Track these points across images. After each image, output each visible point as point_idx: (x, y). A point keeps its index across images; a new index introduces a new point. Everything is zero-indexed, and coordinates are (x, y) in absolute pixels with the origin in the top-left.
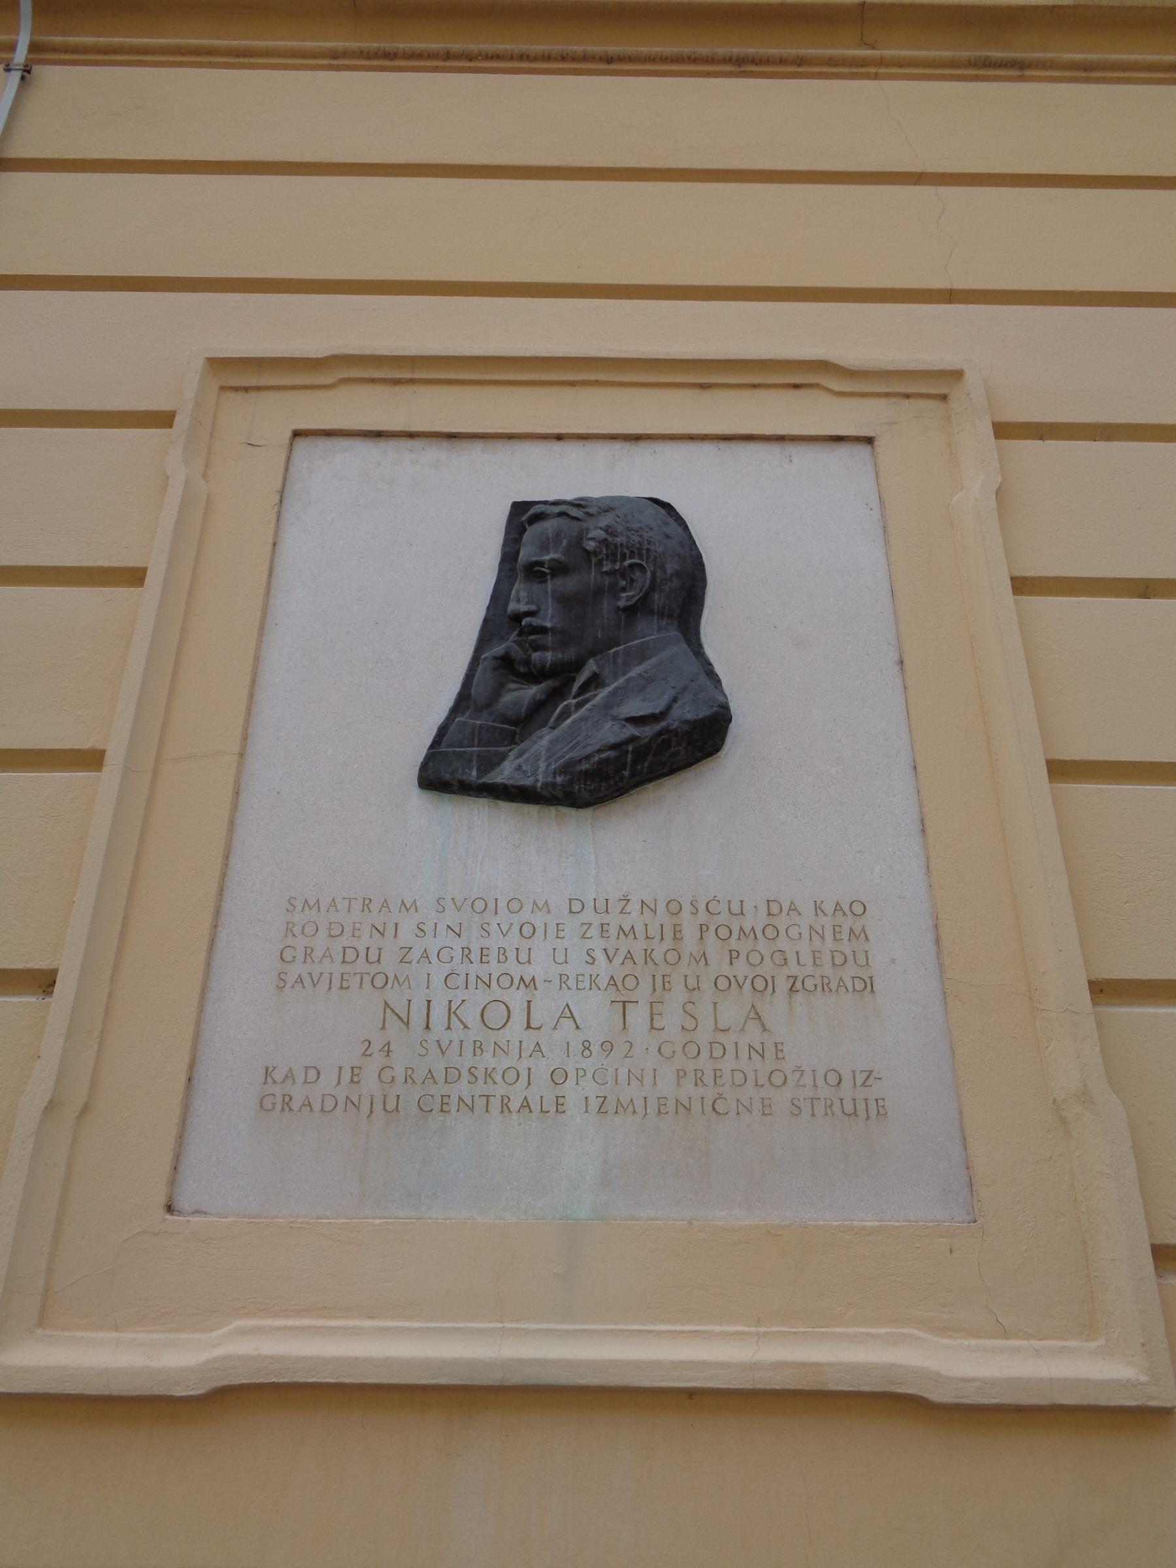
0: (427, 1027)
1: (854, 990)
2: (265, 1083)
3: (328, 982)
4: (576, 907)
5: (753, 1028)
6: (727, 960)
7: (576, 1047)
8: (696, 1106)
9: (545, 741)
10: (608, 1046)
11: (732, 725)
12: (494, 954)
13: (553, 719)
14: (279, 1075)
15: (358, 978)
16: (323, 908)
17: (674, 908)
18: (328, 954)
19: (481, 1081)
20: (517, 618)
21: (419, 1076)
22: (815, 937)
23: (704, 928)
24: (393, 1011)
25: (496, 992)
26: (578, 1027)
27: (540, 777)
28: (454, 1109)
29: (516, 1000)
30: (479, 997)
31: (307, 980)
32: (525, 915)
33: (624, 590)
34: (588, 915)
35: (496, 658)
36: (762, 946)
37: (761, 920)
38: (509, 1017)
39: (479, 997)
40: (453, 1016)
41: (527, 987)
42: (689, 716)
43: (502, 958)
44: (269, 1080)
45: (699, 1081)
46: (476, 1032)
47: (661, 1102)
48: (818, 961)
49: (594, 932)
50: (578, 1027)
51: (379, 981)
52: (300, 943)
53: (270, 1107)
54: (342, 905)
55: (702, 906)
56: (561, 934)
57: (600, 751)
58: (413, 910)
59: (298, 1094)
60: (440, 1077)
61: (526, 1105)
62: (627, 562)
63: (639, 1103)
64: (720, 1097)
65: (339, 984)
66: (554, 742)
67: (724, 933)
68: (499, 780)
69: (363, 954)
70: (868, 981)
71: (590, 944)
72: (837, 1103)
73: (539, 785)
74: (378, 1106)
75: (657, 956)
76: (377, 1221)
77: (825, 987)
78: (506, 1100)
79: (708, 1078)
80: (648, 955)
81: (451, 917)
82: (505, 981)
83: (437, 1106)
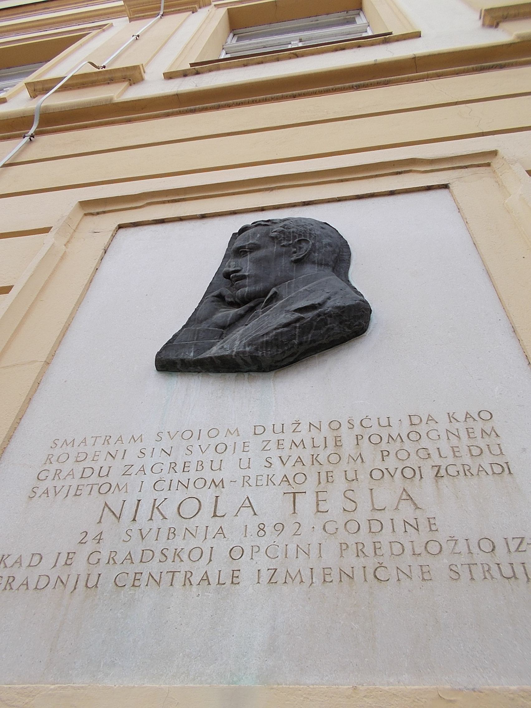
1: (494, 473)
3: (67, 491)
4: (259, 430)
7: (253, 529)
8: (358, 574)
9: (241, 332)
10: (280, 527)
12: (193, 466)
16: (76, 444)
18: (71, 474)
19: (170, 560)
23: (360, 437)
24: (109, 508)
25: (192, 491)
27: (235, 350)
29: (207, 496)
30: (178, 495)
35: (213, 296)
36: (408, 445)
37: (405, 429)
40: (155, 510)
41: (216, 486)
43: (200, 468)
45: (360, 552)
46: (173, 520)
47: (326, 571)
49: (273, 446)
52: (53, 468)
55: (357, 423)
56: (246, 449)
57: (276, 329)
60: (137, 558)
61: (206, 578)
63: (306, 574)
64: (381, 565)
66: (245, 331)
70: (505, 466)
71: (267, 454)
72: (494, 568)
73: (234, 353)
74: (81, 583)
77: (467, 472)
78: (189, 575)
79: (369, 550)
80: (314, 459)
81: (166, 444)
82: (200, 483)
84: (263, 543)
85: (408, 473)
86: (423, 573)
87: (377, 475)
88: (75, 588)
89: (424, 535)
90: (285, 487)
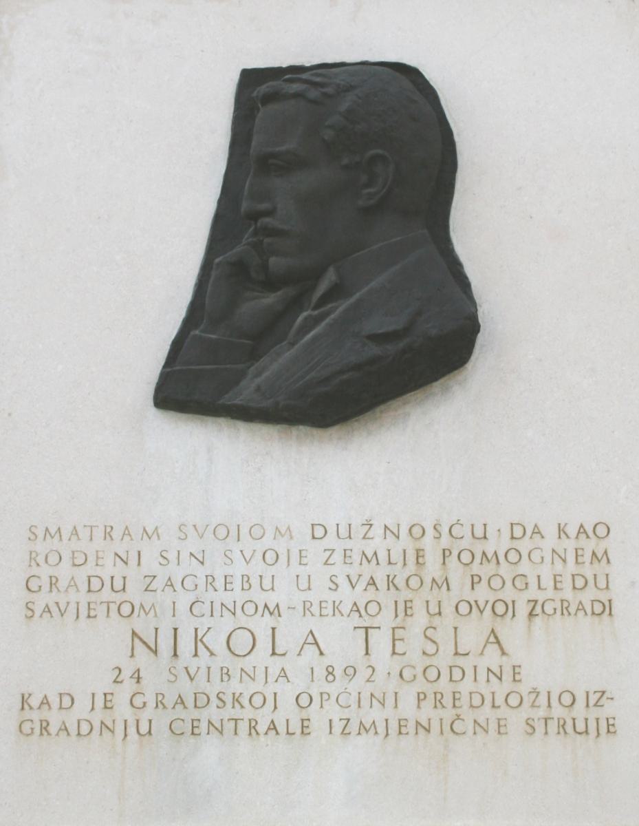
0: (175, 655)
1: (593, 613)
2: (23, 708)
3: (75, 611)
4: (319, 532)
5: (492, 649)
7: (320, 673)
10: (351, 672)
11: (480, 335)
14: (35, 702)
15: (104, 607)
17: (416, 531)
18: (73, 583)
19: (229, 705)
20: (254, 216)
21: (170, 700)
22: (557, 560)
23: (447, 553)
24: (141, 639)
25: (242, 620)
26: (321, 653)
30: (226, 623)
31: (54, 609)
32: (268, 541)
33: (367, 185)
38: (253, 647)
39: (226, 623)
40: (199, 644)
41: (271, 614)
42: (434, 332)
44: (26, 706)
45: (438, 703)
48: (559, 585)
49: (337, 557)
50: (321, 653)
52: (45, 572)
53: (30, 731)
54: (84, 534)
55: (445, 530)
56: (304, 561)
57: (342, 372)
58: (155, 536)
59: (55, 718)
60: (190, 702)
61: (273, 727)
64: (458, 717)
65: (86, 613)
67: (466, 557)
68: (237, 402)
74: (132, 730)
75: (400, 582)
77: (565, 609)
79: (448, 701)
80: (391, 582)
81: (193, 545)
82: (250, 608)
85: (500, 608)
86: (499, 726)
87: (464, 608)
88: (126, 735)
90: (355, 620)
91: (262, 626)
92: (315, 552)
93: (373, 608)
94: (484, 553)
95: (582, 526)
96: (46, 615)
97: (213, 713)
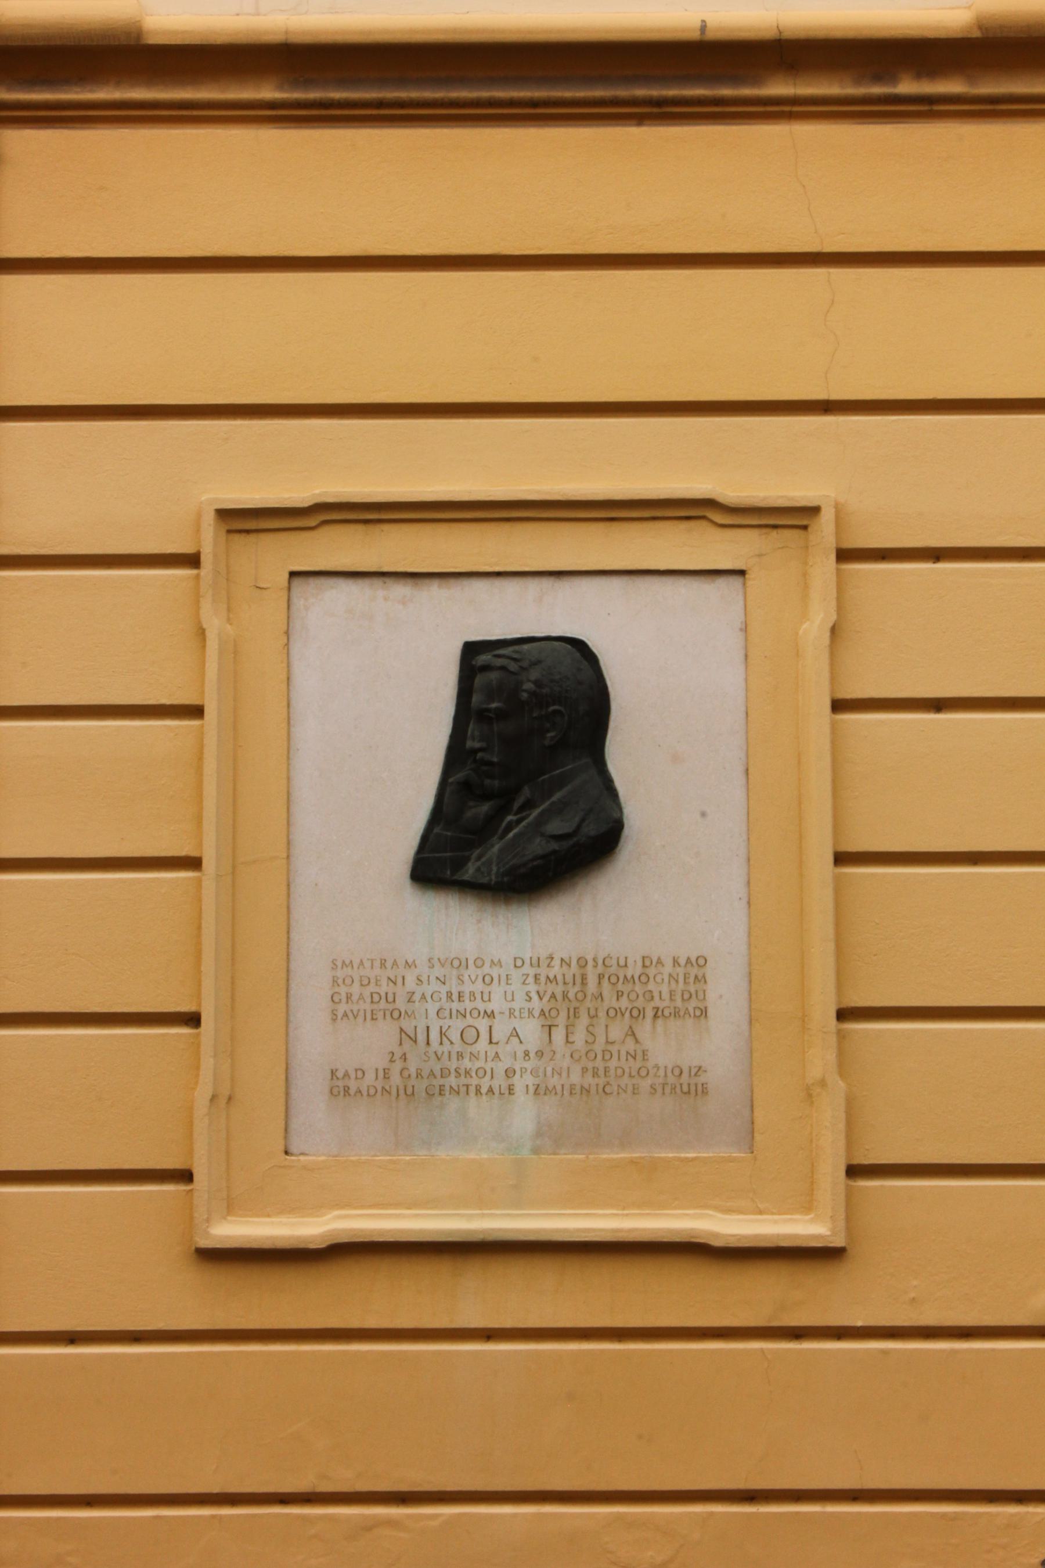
0: (428, 1043)
4: (519, 963)
5: (630, 1040)
6: (615, 997)
7: (520, 1054)
9: (496, 849)
10: (540, 1054)
12: (467, 995)
13: (500, 831)
14: (340, 1074)
15: (382, 1013)
17: (582, 963)
18: (361, 997)
19: (463, 1076)
21: (425, 1073)
22: (673, 982)
25: (469, 1020)
28: (447, 1093)
30: (458, 1024)
31: (350, 1015)
32: (486, 969)
33: (548, 731)
34: (527, 969)
36: (638, 988)
37: (639, 970)
39: (458, 1024)
45: (595, 1074)
46: (458, 1046)
47: (572, 1087)
49: (531, 980)
51: (396, 1014)
52: (343, 990)
54: (367, 964)
59: (353, 1085)
60: (438, 1073)
61: (491, 1090)
62: (552, 708)
63: (559, 1088)
64: (608, 1083)
66: (501, 850)
67: (613, 979)
68: (466, 877)
69: (383, 996)
72: (678, 1087)
74: (402, 1092)
75: (571, 995)
76: (408, 1158)
77: (676, 1014)
79: (601, 1072)
80: (565, 996)
81: (438, 971)
82: (475, 1013)
83: (437, 1091)
84: (529, 1065)
85: (635, 1013)
87: (612, 1013)
89: (639, 1063)
91: (483, 1024)
92: (516, 975)
93: (554, 1013)
94: (625, 977)
95: (689, 958)
96: (345, 1018)
97: (452, 1081)
